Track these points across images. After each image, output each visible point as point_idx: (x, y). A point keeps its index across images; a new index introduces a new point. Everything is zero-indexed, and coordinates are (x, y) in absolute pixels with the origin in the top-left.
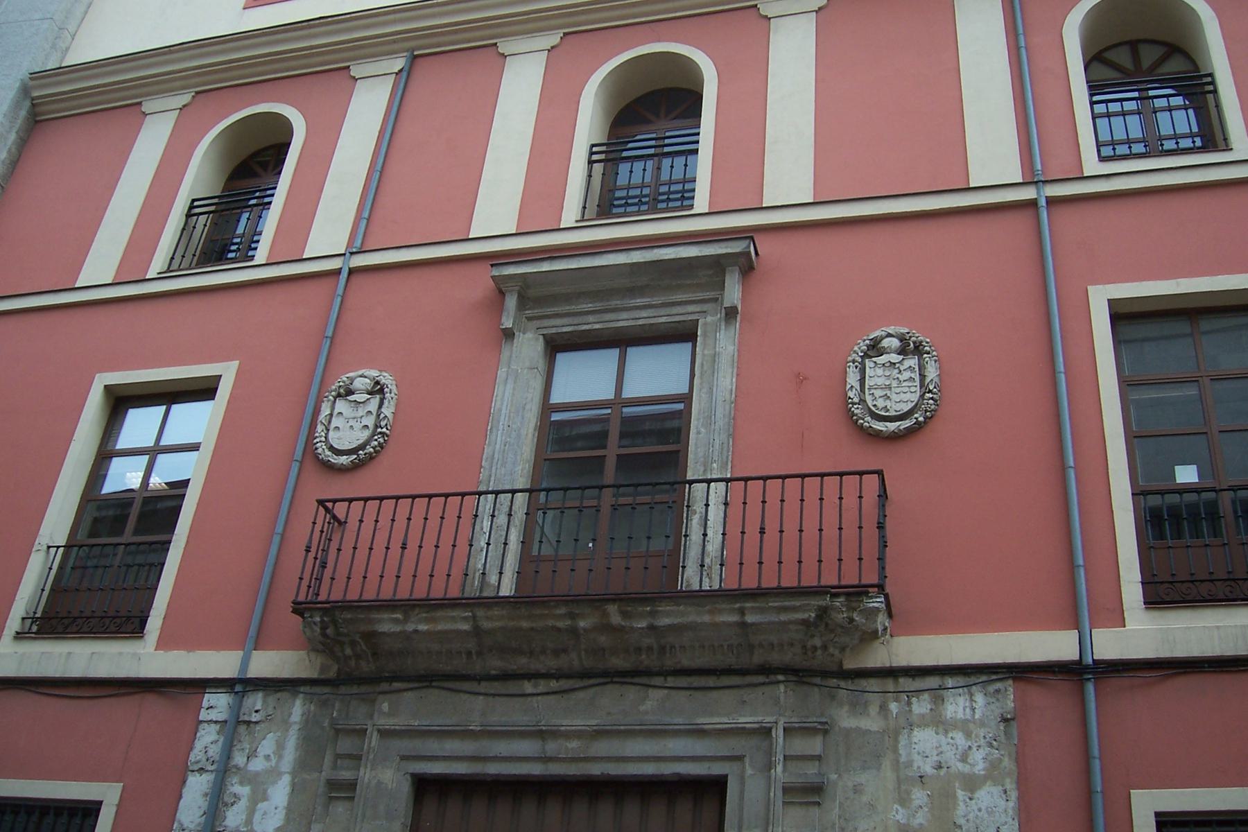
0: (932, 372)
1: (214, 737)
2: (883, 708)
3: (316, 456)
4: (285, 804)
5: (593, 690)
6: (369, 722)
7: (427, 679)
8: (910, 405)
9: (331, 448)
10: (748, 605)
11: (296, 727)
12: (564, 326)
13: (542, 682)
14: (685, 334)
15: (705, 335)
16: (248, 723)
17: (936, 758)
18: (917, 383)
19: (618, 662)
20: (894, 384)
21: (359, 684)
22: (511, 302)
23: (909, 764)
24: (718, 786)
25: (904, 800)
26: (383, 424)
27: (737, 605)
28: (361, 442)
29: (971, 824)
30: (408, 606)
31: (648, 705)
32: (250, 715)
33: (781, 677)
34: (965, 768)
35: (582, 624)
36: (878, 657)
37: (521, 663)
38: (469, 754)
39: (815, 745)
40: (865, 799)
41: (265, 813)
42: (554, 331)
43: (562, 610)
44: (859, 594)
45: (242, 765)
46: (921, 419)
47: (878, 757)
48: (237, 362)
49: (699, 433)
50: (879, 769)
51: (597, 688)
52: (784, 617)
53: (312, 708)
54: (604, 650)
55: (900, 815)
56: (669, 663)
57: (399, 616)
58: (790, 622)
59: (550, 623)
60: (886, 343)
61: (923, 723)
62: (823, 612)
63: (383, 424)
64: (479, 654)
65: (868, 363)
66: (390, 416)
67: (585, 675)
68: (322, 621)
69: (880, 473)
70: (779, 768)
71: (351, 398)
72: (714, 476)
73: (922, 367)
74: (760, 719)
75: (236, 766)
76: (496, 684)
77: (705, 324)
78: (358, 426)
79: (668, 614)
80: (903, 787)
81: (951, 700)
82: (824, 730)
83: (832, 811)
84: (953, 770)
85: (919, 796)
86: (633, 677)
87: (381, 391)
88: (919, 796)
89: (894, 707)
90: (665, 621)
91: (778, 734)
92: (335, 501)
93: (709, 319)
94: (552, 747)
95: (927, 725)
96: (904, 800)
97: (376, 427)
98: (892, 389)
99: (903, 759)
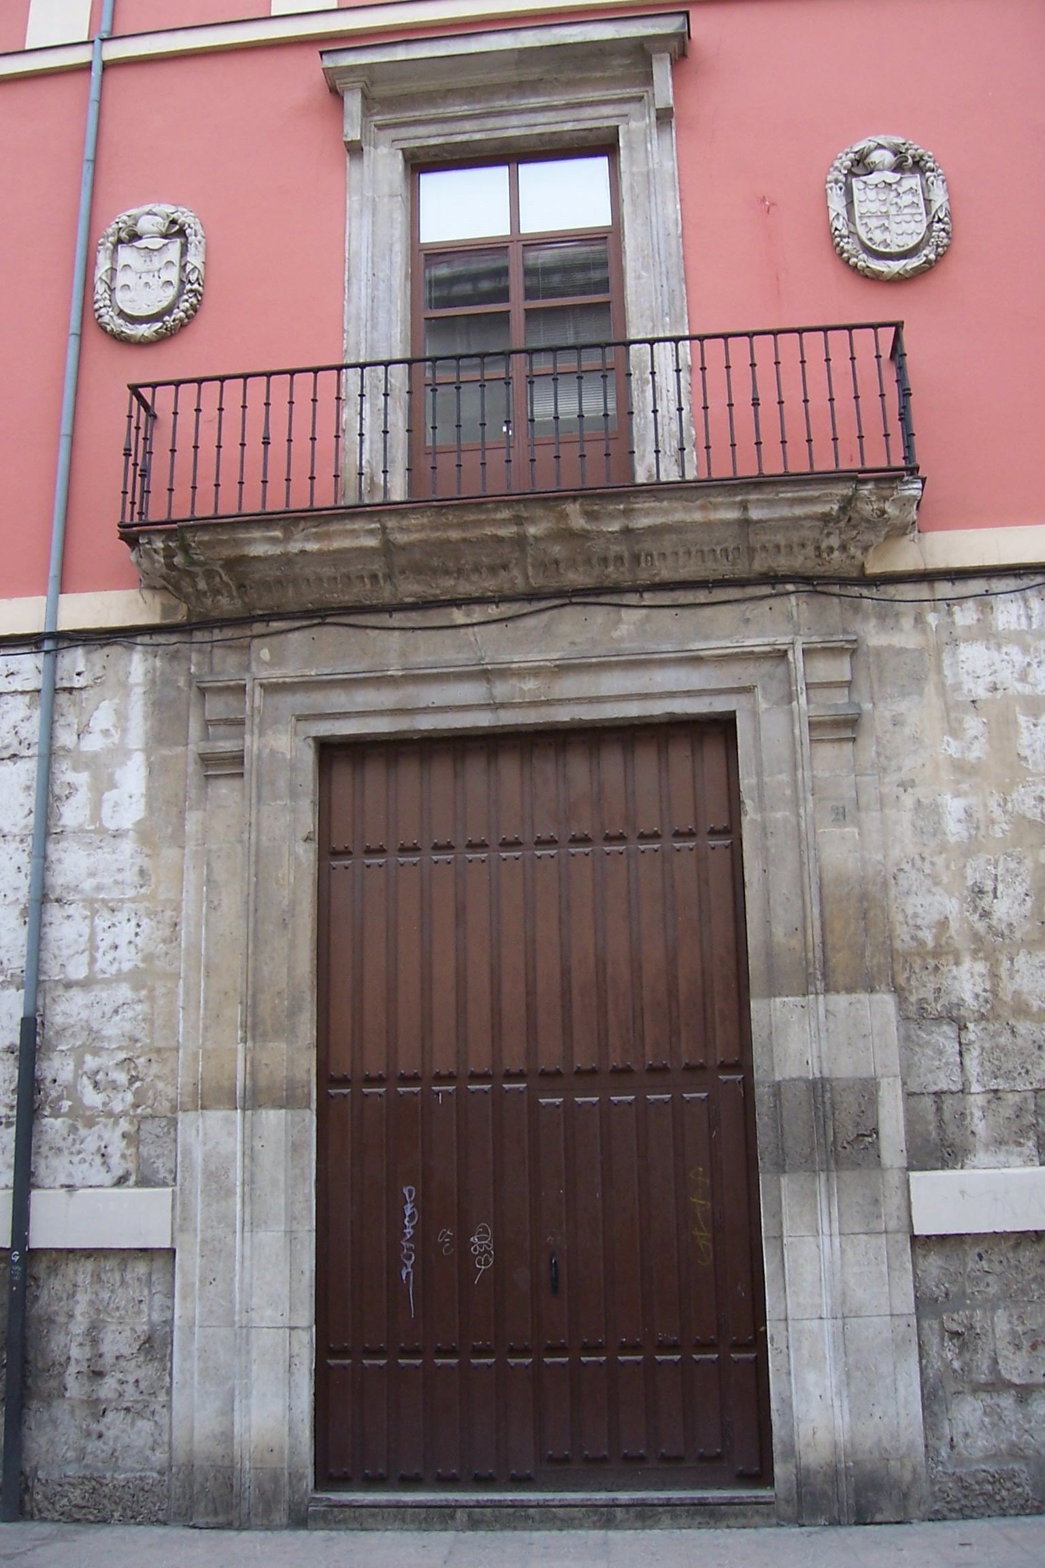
0: (939, 197)
1: (24, 712)
2: (919, 619)
4: (144, 791)
5: (548, 614)
6: (247, 677)
7: (319, 615)
8: (917, 239)
9: (122, 314)
10: (753, 497)
11: (139, 691)
12: (430, 137)
13: (477, 608)
14: (603, 145)
15: (630, 148)
16: (70, 690)
17: (989, 679)
18: (923, 210)
19: (576, 578)
20: (893, 210)
21: (221, 628)
22: (353, 103)
23: (958, 687)
24: (724, 726)
25: (955, 731)
26: (193, 277)
27: (739, 498)
28: (165, 304)
29: (1038, 754)
30: (289, 520)
31: (623, 630)
32: (71, 679)
33: (790, 587)
34: (1027, 689)
35: (532, 530)
36: (906, 556)
37: (447, 585)
38: (392, 707)
39: (840, 669)
40: (907, 731)
41: (116, 804)
42: (417, 143)
43: (505, 514)
44: (892, 479)
45: (71, 746)
46: (932, 256)
47: (919, 679)
49: (639, 277)
50: (921, 694)
51: (555, 612)
52: (799, 511)
53: (158, 663)
54: (557, 562)
55: (953, 748)
56: (644, 577)
57: (278, 534)
58: (807, 517)
59: (488, 531)
60: (876, 157)
61: (971, 638)
62: (847, 503)
63: (193, 277)
64: (388, 577)
65: (856, 184)
66: (200, 266)
67: (532, 596)
68: (167, 548)
69: (898, 326)
70: (803, 699)
72: (661, 335)
73: (926, 189)
74: (771, 640)
75: (63, 748)
76: (413, 615)
77: (628, 132)
78: (155, 282)
79: (647, 513)
80: (953, 715)
81: (1001, 608)
82: (852, 650)
83: (868, 750)
84: (1010, 692)
85: (973, 724)
86: (598, 595)
87: (181, 233)
88: (973, 724)
89: (932, 619)
90: (643, 522)
91: (796, 657)
92: (154, 386)
93: (633, 125)
94: (502, 690)
95: (975, 639)
96: (955, 731)
97: (182, 282)
98: (891, 216)
99: (949, 682)
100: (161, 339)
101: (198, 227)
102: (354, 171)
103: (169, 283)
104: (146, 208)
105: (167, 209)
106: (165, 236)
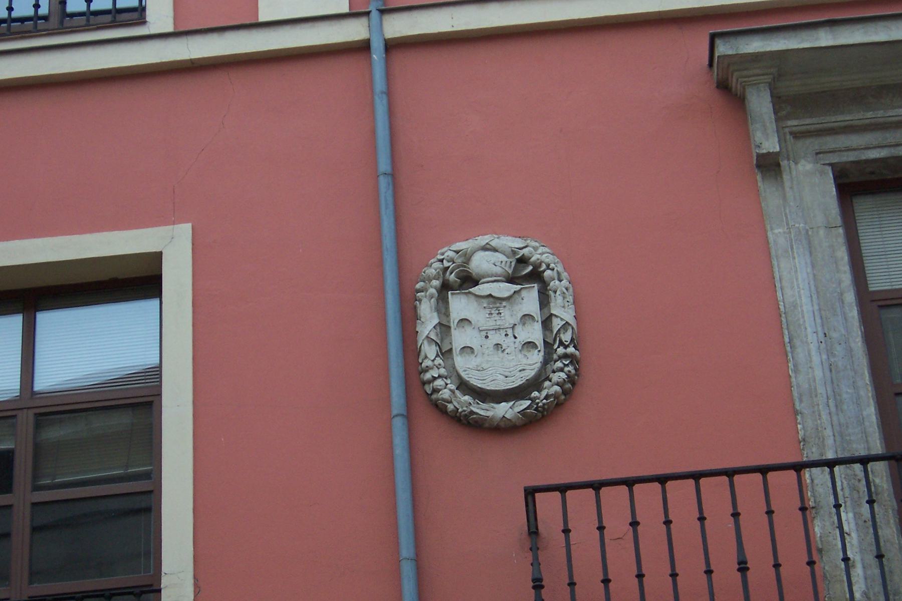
3: (439, 408)
9: (464, 386)
12: (869, 148)
22: (760, 104)
26: (566, 337)
28: (530, 374)
42: (851, 157)
48: (188, 226)
66: (572, 322)
71: (479, 290)
87: (536, 276)
101: (560, 268)
102: (770, 196)
103: (530, 345)
105: (517, 243)
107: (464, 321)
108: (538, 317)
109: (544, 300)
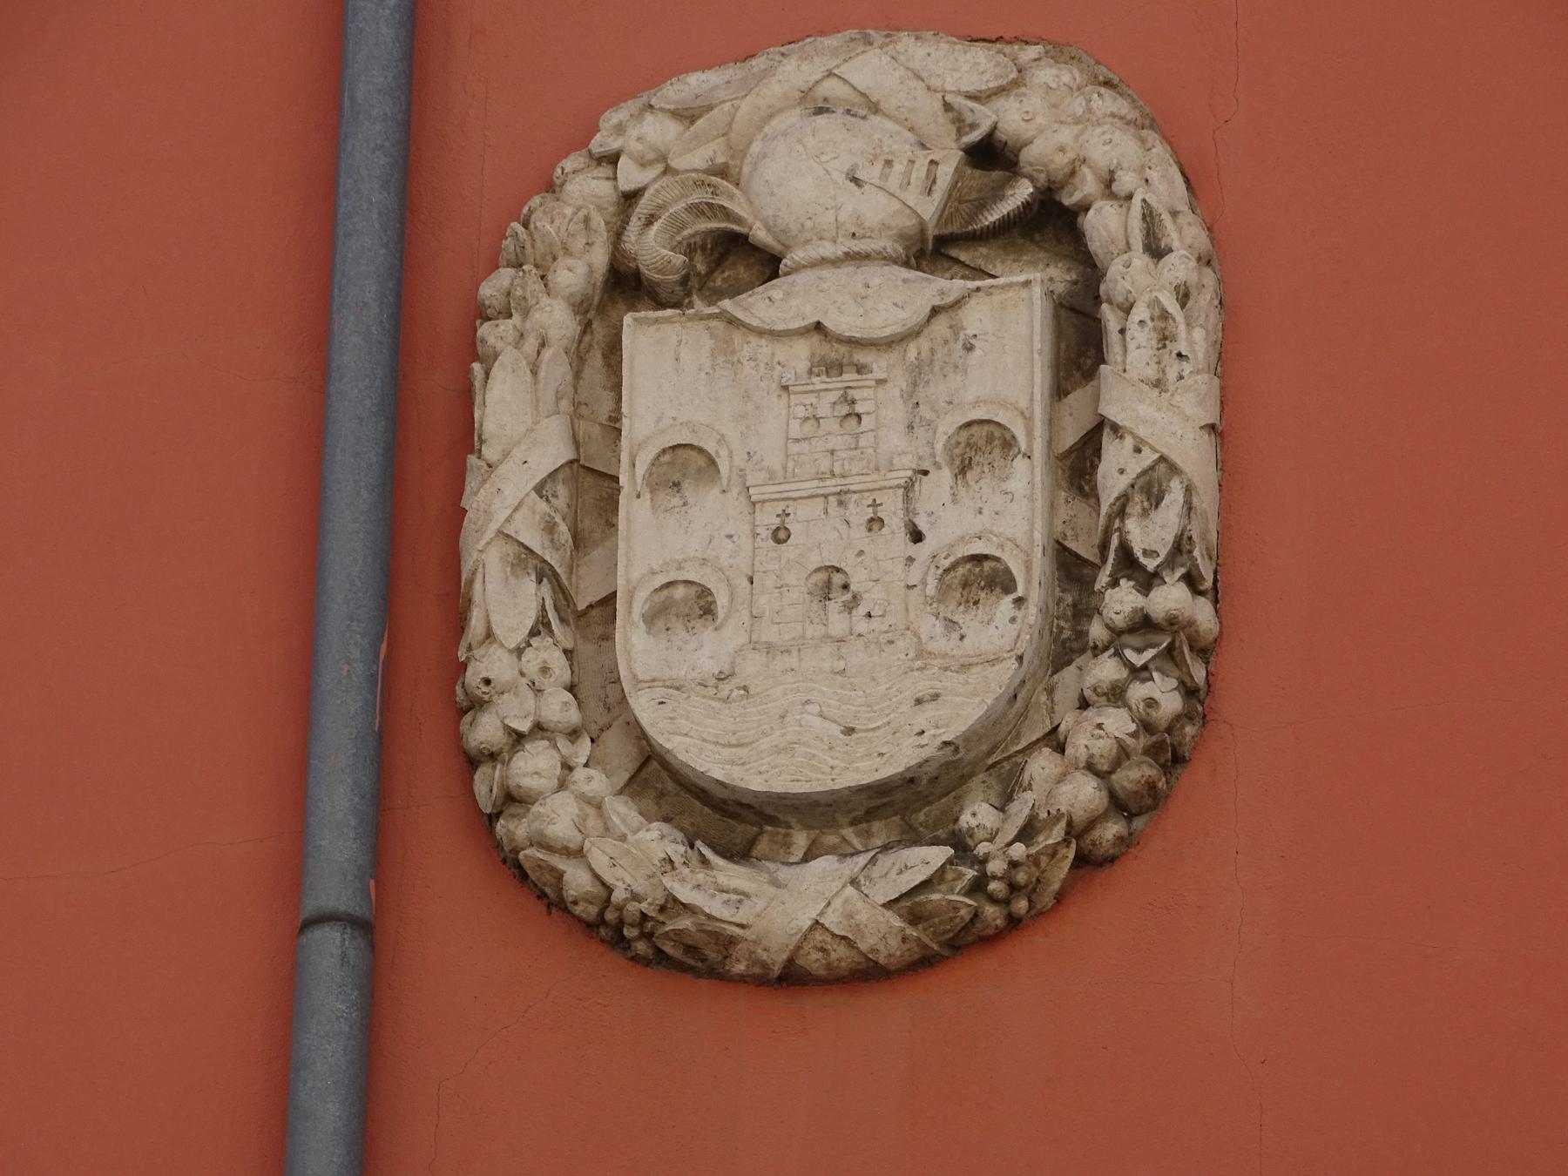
3: (530, 884)
9: (658, 780)
28: (963, 709)
63: (1150, 535)
66: (1195, 456)
71: (764, 305)
78: (886, 571)
87: (1052, 222)
97: (1071, 570)
100: (946, 944)
101: (1164, 186)
103: (982, 576)
104: (795, 70)
105: (967, 67)
106: (932, 250)
107: (686, 465)
108: (1033, 438)
109: (1080, 344)
